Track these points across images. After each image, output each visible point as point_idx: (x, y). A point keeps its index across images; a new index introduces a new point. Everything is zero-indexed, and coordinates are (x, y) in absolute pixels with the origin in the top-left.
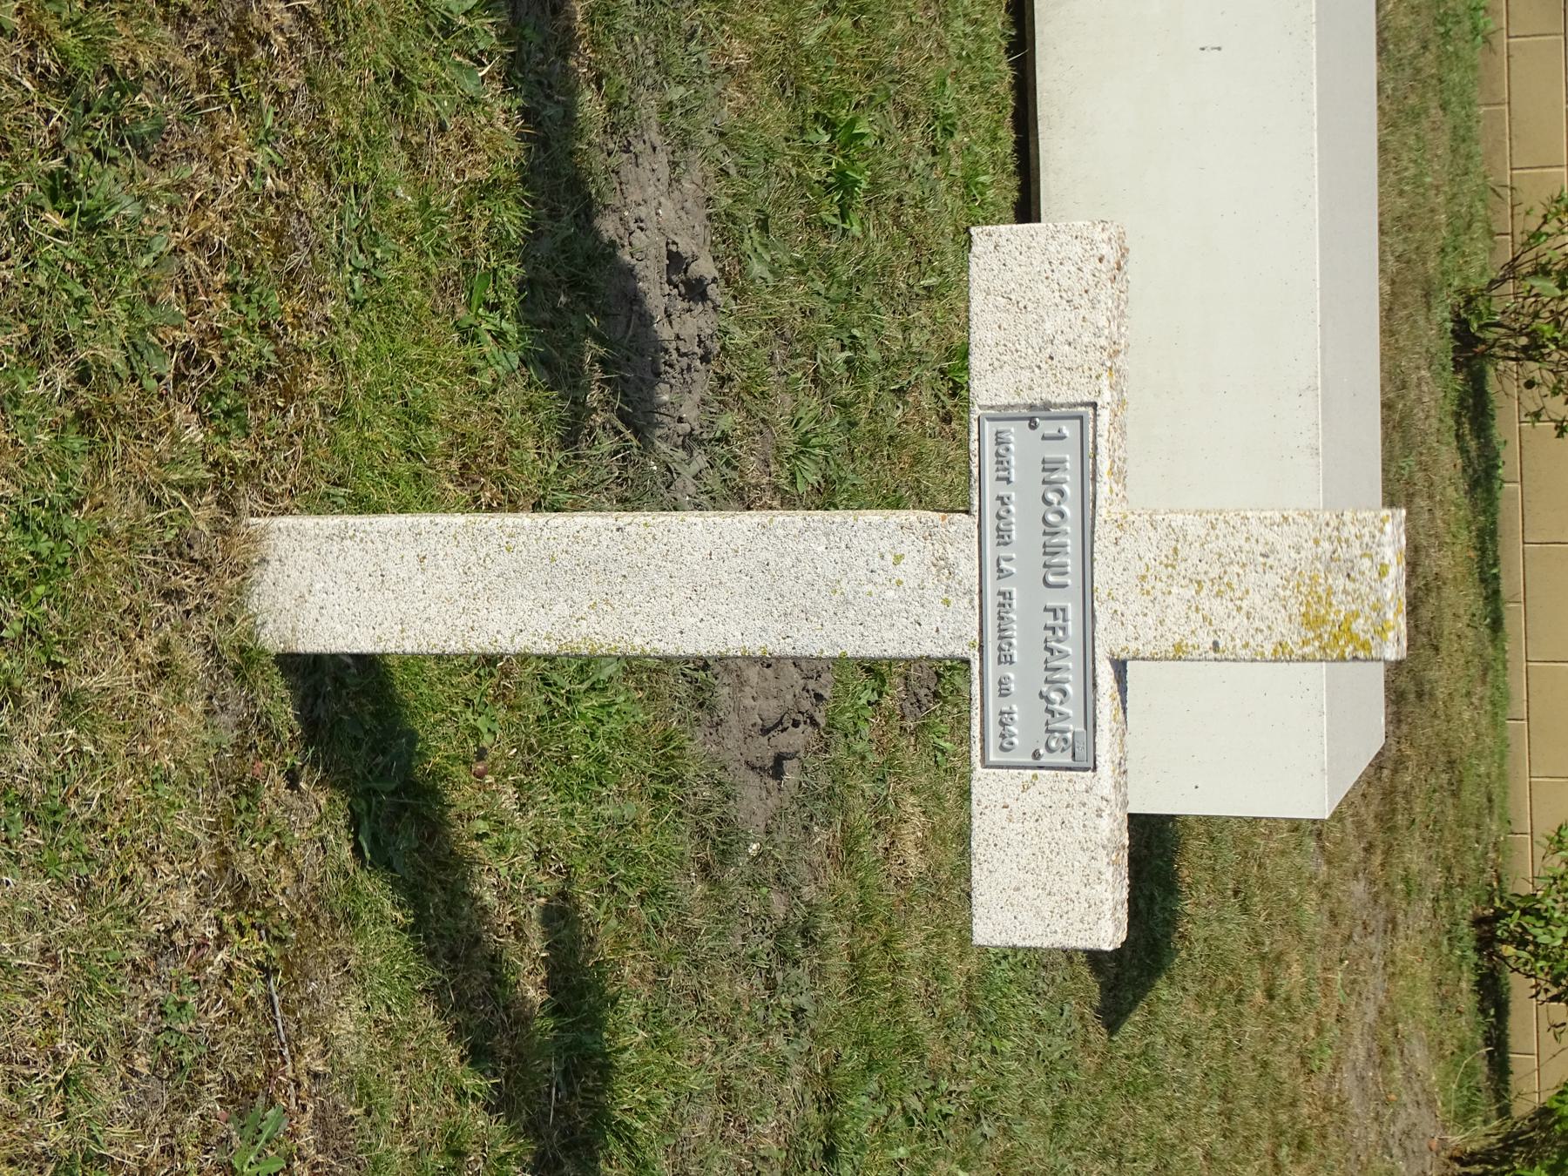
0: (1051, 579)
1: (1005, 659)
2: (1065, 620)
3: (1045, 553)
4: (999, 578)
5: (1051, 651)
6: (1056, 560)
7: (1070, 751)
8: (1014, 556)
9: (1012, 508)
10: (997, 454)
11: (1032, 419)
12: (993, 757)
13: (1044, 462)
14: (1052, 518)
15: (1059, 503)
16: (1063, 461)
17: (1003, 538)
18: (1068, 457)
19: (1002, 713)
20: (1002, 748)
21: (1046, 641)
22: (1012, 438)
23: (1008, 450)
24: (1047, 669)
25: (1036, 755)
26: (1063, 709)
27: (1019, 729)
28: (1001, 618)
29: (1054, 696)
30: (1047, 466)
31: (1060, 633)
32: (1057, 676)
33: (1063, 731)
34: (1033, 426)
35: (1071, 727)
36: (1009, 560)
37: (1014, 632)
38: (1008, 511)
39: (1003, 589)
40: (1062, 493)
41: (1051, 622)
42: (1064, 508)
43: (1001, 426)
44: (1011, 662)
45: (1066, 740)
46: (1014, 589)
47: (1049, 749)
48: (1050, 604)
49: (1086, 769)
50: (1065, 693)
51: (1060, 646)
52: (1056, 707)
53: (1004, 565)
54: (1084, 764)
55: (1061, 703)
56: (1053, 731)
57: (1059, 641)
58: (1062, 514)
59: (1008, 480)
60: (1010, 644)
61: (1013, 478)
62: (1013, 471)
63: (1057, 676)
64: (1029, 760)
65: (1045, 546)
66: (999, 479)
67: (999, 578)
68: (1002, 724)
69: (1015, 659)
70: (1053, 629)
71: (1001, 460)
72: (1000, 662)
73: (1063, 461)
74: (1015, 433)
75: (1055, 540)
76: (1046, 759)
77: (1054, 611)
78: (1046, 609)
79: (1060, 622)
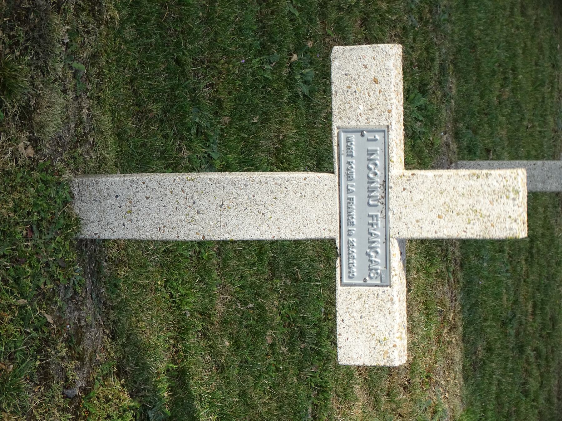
0: (371, 203)
1: (351, 224)
2: (377, 220)
3: (368, 154)
4: (348, 193)
5: (371, 234)
6: (372, 194)
7: (379, 278)
8: (354, 184)
9: (353, 166)
10: (347, 146)
11: (362, 132)
12: (345, 281)
13: (368, 151)
14: (371, 176)
15: (375, 169)
16: (376, 151)
17: (349, 177)
18: (378, 148)
19: (349, 230)
20: (349, 277)
21: (369, 230)
22: (354, 140)
23: (352, 144)
24: (369, 242)
25: (365, 280)
26: (376, 260)
27: (357, 269)
28: (348, 208)
29: (372, 254)
30: (369, 152)
31: (375, 227)
32: (373, 245)
33: (376, 270)
34: (362, 135)
35: (380, 267)
36: (352, 186)
37: (354, 213)
38: (352, 167)
39: (349, 197)
40: (376, 165)
41: (371, 221)
42: (376, 171)
43: (349, 135)
44: (353, 225)
45: (377, 273)
46: (354, 197)
47: (371, 278)
48: (371, 214)
49: (387, 286)
50: (377, 253)
51: (376, 232)
52: (373, 259)
53: (349, 188)
54: (386, 284)
55: (376, 257)
56: (372, 269)
57: (374, 230)
58: (375, 174)
59: (352, 156)
60: (353, 218)
61: (354, 155)
62: (353, 151)
63: (373, 245)
64: (362, 282)
65: (368, 188)
66: (348, 155)
67: (348, 193)
68: (350, 268)
69: (355, 223)
70: (372, 225)
71: (348, 148)
72: (348, 225)
73: (376, 151)
74: (354, 137)
75: (372, 185)
76: (369, 281)
77: (372, 216)
78: (369, 216)
79: (375, 221)
